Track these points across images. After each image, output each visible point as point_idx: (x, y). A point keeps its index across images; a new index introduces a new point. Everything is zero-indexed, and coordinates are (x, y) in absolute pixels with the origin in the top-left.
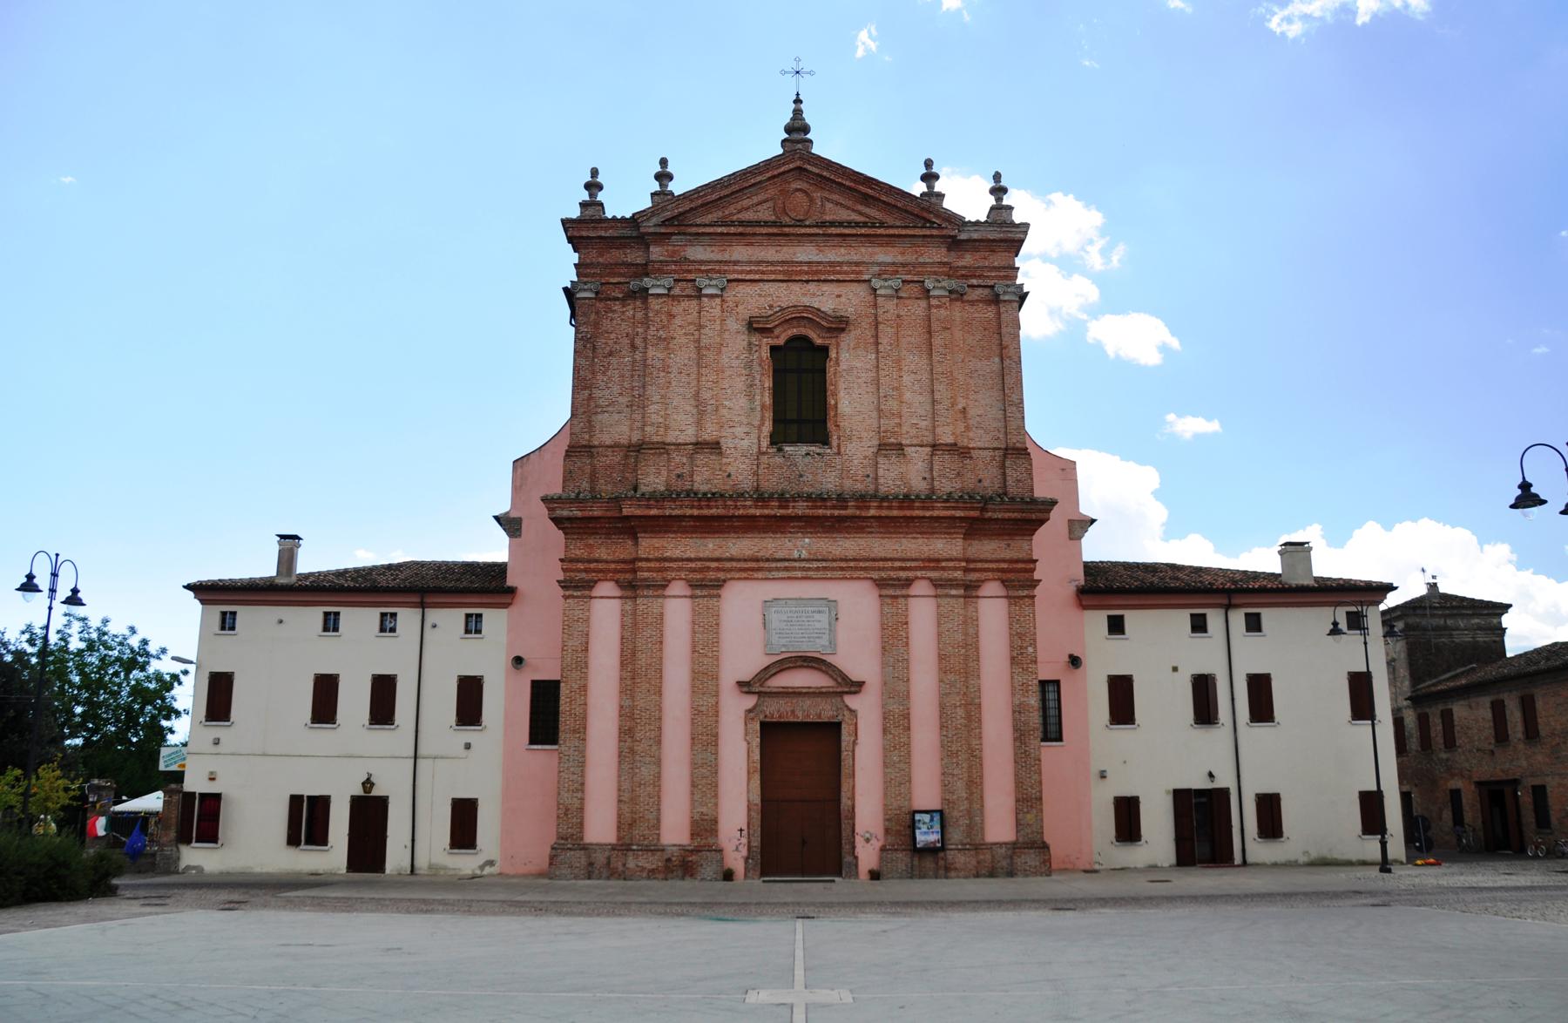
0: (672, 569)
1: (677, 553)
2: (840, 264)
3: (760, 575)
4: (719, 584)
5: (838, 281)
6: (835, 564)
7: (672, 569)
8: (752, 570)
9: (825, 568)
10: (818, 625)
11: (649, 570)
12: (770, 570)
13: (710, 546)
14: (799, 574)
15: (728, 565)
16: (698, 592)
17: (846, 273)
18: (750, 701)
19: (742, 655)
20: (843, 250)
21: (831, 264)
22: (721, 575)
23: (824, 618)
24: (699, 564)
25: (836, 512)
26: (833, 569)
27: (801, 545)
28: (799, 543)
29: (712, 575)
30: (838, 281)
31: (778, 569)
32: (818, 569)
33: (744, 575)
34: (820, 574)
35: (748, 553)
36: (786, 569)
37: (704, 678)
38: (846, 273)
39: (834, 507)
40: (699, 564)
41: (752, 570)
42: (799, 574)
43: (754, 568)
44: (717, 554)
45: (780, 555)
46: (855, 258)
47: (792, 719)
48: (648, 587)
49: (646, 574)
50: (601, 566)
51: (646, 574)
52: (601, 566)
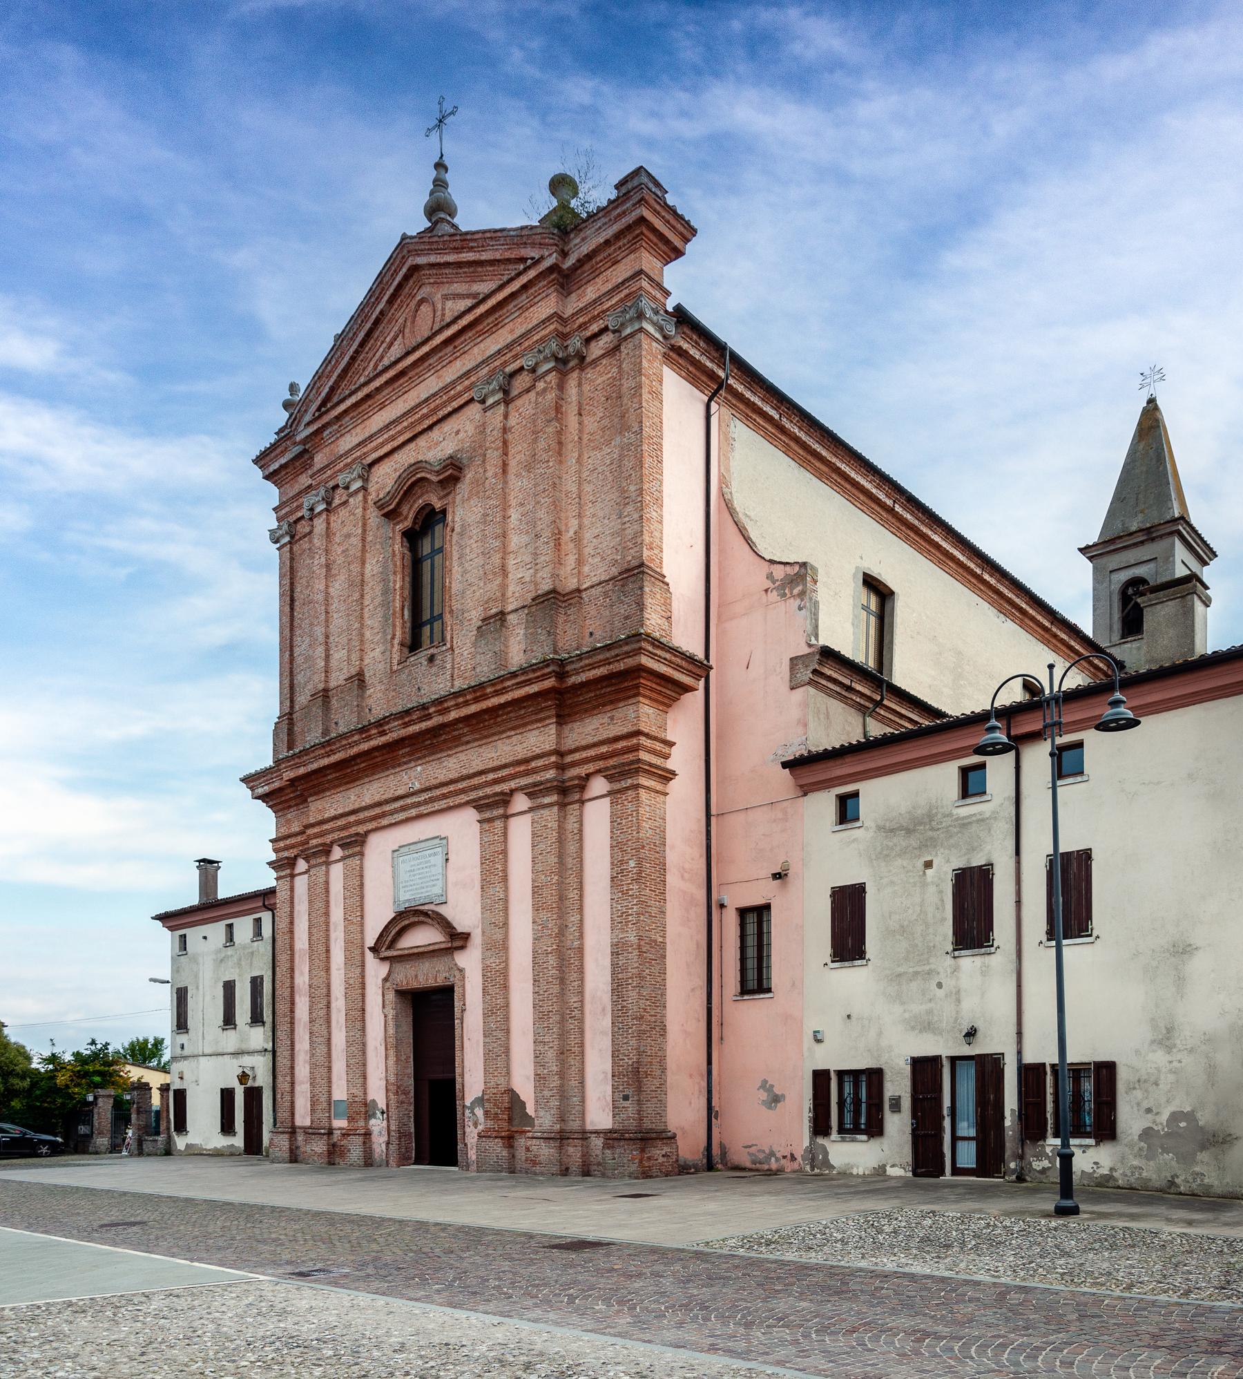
32: (425, 802)
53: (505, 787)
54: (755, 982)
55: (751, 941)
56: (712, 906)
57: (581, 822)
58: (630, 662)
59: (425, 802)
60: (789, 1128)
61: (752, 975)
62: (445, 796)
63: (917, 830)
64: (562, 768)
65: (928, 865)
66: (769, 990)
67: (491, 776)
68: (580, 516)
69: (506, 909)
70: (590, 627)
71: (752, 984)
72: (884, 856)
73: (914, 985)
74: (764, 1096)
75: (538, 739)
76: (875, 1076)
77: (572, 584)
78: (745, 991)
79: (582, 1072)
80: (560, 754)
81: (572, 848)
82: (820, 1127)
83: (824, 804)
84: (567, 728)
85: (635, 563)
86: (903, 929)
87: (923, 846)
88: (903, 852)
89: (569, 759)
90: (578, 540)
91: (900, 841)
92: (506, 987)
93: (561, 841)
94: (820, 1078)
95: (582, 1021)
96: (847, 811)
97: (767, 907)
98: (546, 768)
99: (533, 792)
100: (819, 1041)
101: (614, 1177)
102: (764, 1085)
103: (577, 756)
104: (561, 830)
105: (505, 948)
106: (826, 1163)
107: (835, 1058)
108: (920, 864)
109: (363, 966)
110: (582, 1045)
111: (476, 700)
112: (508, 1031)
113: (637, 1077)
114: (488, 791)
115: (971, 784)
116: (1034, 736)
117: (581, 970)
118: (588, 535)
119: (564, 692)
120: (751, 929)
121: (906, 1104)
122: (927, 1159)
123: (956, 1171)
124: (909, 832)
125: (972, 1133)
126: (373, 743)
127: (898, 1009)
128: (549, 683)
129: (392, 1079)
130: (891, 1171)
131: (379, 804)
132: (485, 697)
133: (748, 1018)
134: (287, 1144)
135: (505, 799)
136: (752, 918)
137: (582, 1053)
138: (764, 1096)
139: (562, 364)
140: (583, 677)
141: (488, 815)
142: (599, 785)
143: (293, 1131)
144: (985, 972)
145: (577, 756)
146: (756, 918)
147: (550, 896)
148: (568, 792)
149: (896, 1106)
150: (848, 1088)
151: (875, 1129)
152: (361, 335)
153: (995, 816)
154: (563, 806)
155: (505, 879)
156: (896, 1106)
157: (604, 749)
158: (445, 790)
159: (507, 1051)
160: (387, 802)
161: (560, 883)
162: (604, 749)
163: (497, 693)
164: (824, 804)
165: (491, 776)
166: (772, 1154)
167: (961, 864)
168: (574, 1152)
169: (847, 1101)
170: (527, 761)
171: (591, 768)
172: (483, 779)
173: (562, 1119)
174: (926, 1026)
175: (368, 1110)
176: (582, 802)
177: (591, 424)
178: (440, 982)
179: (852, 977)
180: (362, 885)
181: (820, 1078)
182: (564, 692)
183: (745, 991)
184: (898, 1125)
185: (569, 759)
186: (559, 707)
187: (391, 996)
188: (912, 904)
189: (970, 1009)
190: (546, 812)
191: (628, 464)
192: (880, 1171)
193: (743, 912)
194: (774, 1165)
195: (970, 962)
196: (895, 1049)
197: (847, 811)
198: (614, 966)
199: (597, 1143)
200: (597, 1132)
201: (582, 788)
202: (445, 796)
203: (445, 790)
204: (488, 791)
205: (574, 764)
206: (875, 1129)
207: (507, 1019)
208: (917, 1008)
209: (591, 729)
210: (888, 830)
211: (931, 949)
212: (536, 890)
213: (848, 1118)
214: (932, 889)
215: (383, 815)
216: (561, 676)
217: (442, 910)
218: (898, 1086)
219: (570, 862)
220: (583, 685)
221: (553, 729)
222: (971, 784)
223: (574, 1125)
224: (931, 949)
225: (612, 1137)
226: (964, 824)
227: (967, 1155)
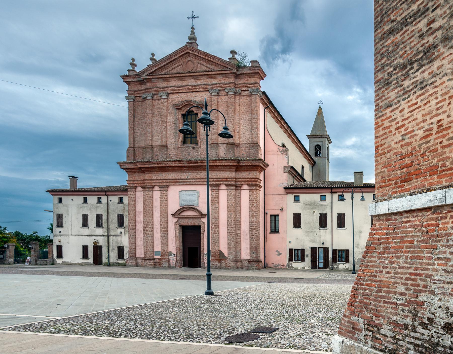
0: (154, 183)
1: (155, 178)
2: (201, 85)
3: (177, 184)
4: (167, 187)
5: (201, 91)
6: (197, 180)
7: (154, 183)
8: (175, 182)
9: (195, 182)
10: (194, 198)
11: (148, 183)
12: (180, 182)
13: (164, 176)
14: (188, 183)
15: (168, 181)
16: (161, 189)
17: (203, 88)
18: (176, 220)
19: (173, 207)
20: (202, 81)
21: (199, 85)
22: (167, 184)
23: (196, 196)
24: (161, 181)
25: (195, 164)
26: (197, 182)
27: (188, 175)
28: (188, 174)
29: (164, 184)
30: (201, 91)
31: (182, 182)
32: (193, 182)
33: (173, 184)
34: (194, 183)
35: (174, 178)
36: (184, 182)
37: (164, 214)
38: (203, 88)
39: (194, 163)
40: (161, 181)
41: (175, 182)
42: (188, 183)
43: (176, 182)
44: (166, 178)
45: (182, 178)
46: (205, 83)
47: (187, 224)
48: (148, 188)
49: (148, 184)
50: (137, 182)
51: (148, 184)
52: (137, 182)
53: (219, 183)
54: (275, 230)
55: (273, 222)
56: (265, 214)
57: (240, 194)
58: (257, 164)
59: (193, 182)
60: (284, 259)
61: (273, 229)
62: (199, 181)
63: (311, 205)
64: (236, 182)
65: (314, 212)
66: (278, 232)
67: (215, 180)
68: (240, 128)
69: (219, 210)
70: (243, 153)
71: (273, 231)
72: (305, 209)
73: (311, 234)
74: (277, 253)
75: (230, 174)
76: (303, 250)
77: (237, 142)
78: (271, 232)
79: (240, 247)
80: (236, 179)
81: (238, 199)
82: (291, 259)
83: (292, 197)
84: (237, 173)
85: (255, 142)
86: (309, 223)
87: (313, 208)
88: (309, 209)
89: (238, 180)
90: (239, 132)
91: (308, 206)
92: (218, 227)
93: (235, 197)
94: (291, 250)
95: (240, 236)
96: (297, 199)
97: (278, 215)
98: (232, 181)
99: (227, 186)
100: (290, 243)
101: (251, 270)
102: (277, 251)
103: (240, 180)
104: (236, 195)
105: (218, 218)
106: (292, 266)
107: (294, 246)
108: (312, 211)
109: (167, 218)
110: (240, 242)
111: (213, 163)
112: (219, 237)
113: (255, 249)
114: (214, 183)
115: (323, 198)
116: (336, 192)
117: (240, 225)
118: (242, 133)
119: (238, 167)
120: (273, 219)
121: (310, 256)
122: (314, 266)
123: (319, 268)
124: (310, 205)
125: (322, 261)
126: (176, 165)
127: (308, 238)
128: (236, 164)
129: (178, 246)
130: (306, 268)
131: (176, 179)
132: (217, 163)
133: (273, 237)
134: (134, 262)
135: (219, 186)
136: (273, 217)
137: (240, 243)
138: (277, 253)
139: (235, 93)
140: (244, 164)
141: (213, 188)
142: (245, 187)
143: (136, 259)
144: (325, 232)
145: (240, 180)
146: (275, 217)
147: (233, 209)
148: (238, 187)
149: (307, 256)
150: (296, 253)
151: (303, 260)
152: (169, 61)
153: (327, 205)
154: (236, 190)
155: (218, 203)
156: (307, 256)
157: (248, 180)
158: (200, 180)
159: (219, 242)
160: (179, 179)
161: (235, 206)
162: (248, 180)
163: (220, 162)
164: (292, 197)
165: (215, 180)
166: (279, 265)
167: (321, 213)
168: (239, 264)
169: (296, 255)
170: (227, 178)
171: (244, 183)
172: (213, 180)
173: (235, 257)
174: (314, 241)
175: (170, 254)
176: (241, 190)
177: (242, 109)
178: (196, 224)
179: (297, 231)
180: (167, 198)
181: (291, 250)
182: (238, 167)
183: (271, 232)
184: (308, 260)
185: (238, 180)
186: (236, 169)
187: (178, 226)
188: (310, 219)
189: (323, 239)
190: (232, 190)
191: (254, 121)
192: (304, 268)
193: (271, 215)
194: (279, 267)
195: (322, 230)
196: (308, 246)
197: (297, 199)
198: (250, 226)
199: (246, 263)
200: (245, 260)
201: (241, 187)
202: (199, 181)
203: (200, 180)
204: (214, 183)
205: (239, 181)
206: (303, 260)
207: (219, 234)
208: (312, 238)
209: (243, 175)
210: (306, 204)
211: (315, 228)
212: (228, 207)
213: (296, 258)
214: (315, 216)
215: (177, 182)
216: (238, 163)
217: (197, 208)
218: (308, 252)
219: (237, 202)
220: (244, 166)
221: (234, 173)
222: (323, 198)
223: (239, 259)
224: (315, 228)
225: (250, 261)
226: (322, 205)
227: (321, 265)
